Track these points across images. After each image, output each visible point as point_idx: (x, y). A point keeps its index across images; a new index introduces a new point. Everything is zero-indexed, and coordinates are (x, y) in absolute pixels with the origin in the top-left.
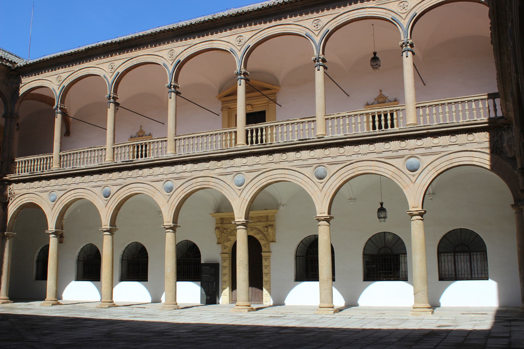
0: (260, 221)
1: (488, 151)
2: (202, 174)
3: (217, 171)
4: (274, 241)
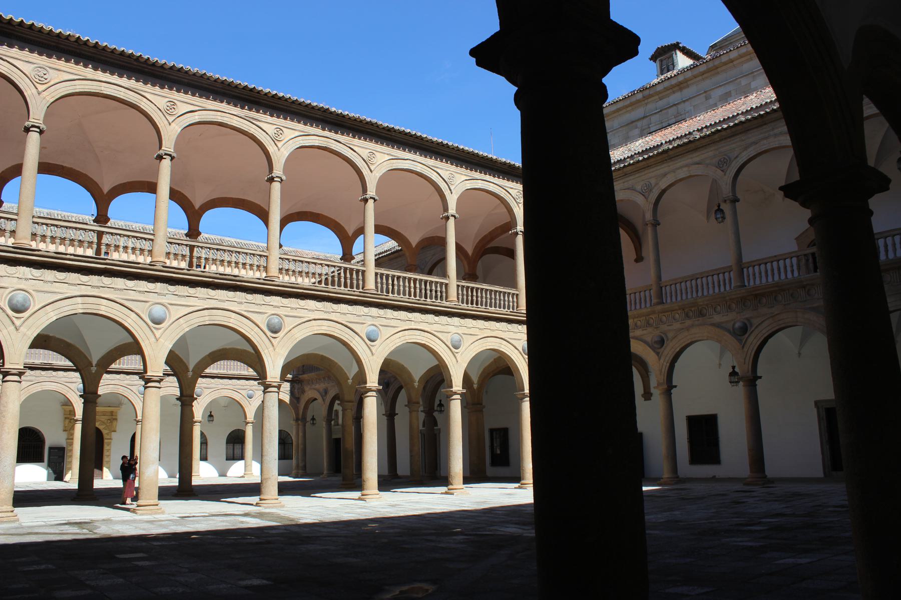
0: (104, 415)
1: (288, 392)
2: (113, 382)
3: (126, 382)
4: (115, 431)
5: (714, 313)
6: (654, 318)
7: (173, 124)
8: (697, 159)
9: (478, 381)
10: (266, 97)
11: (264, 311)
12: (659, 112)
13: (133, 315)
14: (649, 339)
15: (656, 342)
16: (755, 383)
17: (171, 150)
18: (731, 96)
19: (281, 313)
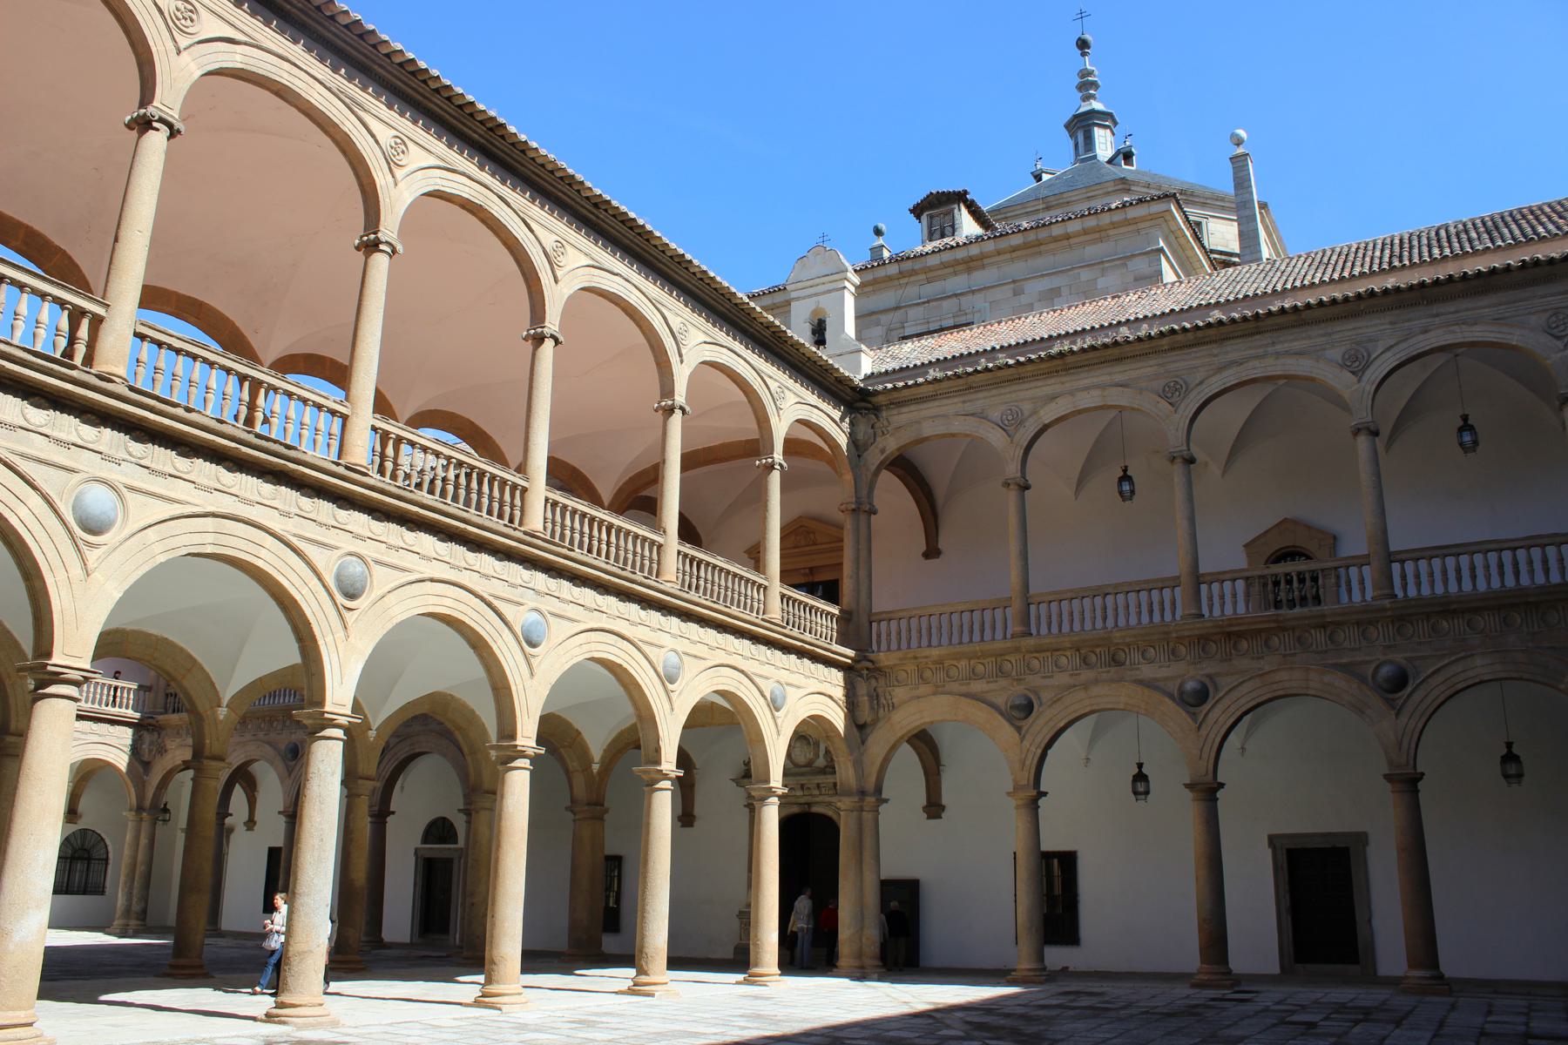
1: (127, 750)
5: (1141, 659)
6: (1014, 662)
7: (184, 54)
8: (1118, 378)
9: (603, 758)
10: (388, 61)
11: (332, 542)
12: (924, 303)
13: (35, 500)
14: (1000, 700)
15: (1013, 707)
16: (1416, 787)
17: (174, 115)
18: (1060, 296)
19: (366, 552)
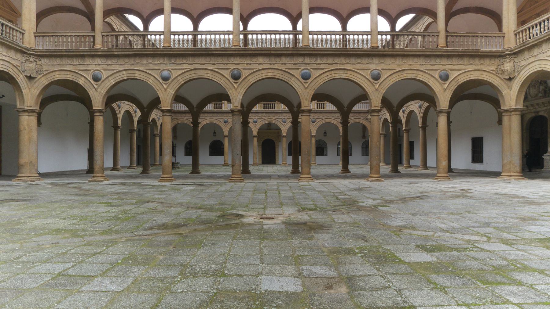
3: (276, 117)
11: (229, 67)
